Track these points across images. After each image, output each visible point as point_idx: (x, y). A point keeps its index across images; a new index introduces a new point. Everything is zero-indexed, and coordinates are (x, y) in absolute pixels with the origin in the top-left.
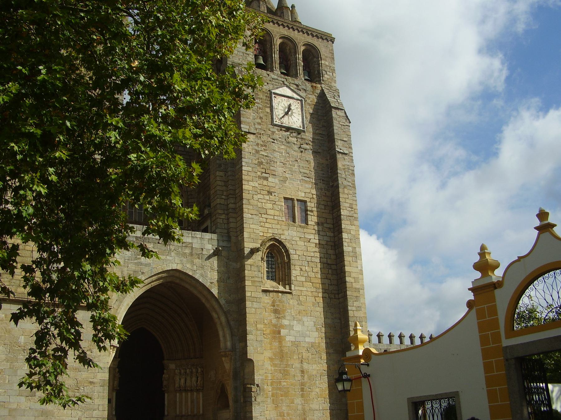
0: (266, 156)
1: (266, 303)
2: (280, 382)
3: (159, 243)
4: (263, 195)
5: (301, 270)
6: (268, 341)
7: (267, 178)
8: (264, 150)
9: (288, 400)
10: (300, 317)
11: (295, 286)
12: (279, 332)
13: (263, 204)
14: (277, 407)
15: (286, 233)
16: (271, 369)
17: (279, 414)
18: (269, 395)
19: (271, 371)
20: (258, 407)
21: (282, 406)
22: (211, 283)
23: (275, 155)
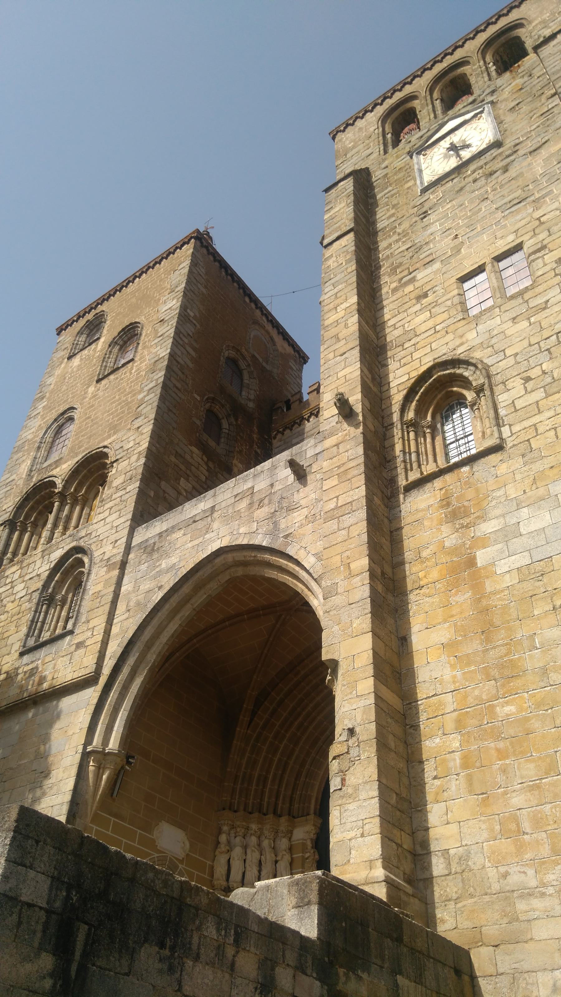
0: (407, 249)
1: (422, 510)
2: (493, 706)
3: (195, 522)
4: (406, 311)
5: (528, 379)
6: (436, 599)
7: (415, 277)
8: (404, 242)
9: (532, 766)
10: (541, 491)
11: (510, 425)
12: (471, 562)
13: (406, 325)
14: (485, 802)
15: (471, 335)
16: (454, 677)
17: (498, 827)
18: (451, 764)
19: (454, 682)
20: (351, 807)
21: (505, 793)
22: (286, 537)
23: (430, 231)
